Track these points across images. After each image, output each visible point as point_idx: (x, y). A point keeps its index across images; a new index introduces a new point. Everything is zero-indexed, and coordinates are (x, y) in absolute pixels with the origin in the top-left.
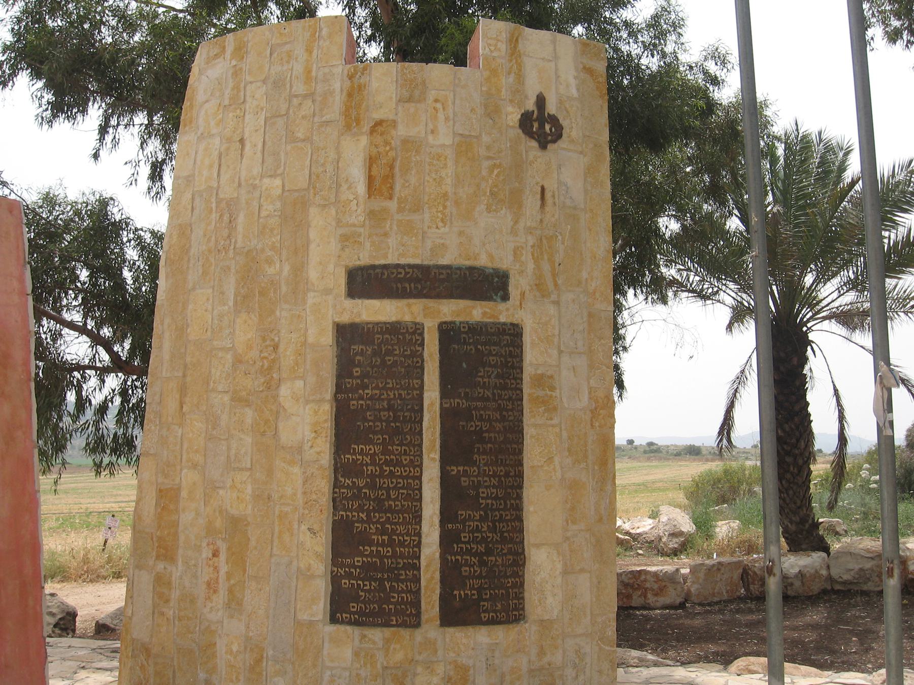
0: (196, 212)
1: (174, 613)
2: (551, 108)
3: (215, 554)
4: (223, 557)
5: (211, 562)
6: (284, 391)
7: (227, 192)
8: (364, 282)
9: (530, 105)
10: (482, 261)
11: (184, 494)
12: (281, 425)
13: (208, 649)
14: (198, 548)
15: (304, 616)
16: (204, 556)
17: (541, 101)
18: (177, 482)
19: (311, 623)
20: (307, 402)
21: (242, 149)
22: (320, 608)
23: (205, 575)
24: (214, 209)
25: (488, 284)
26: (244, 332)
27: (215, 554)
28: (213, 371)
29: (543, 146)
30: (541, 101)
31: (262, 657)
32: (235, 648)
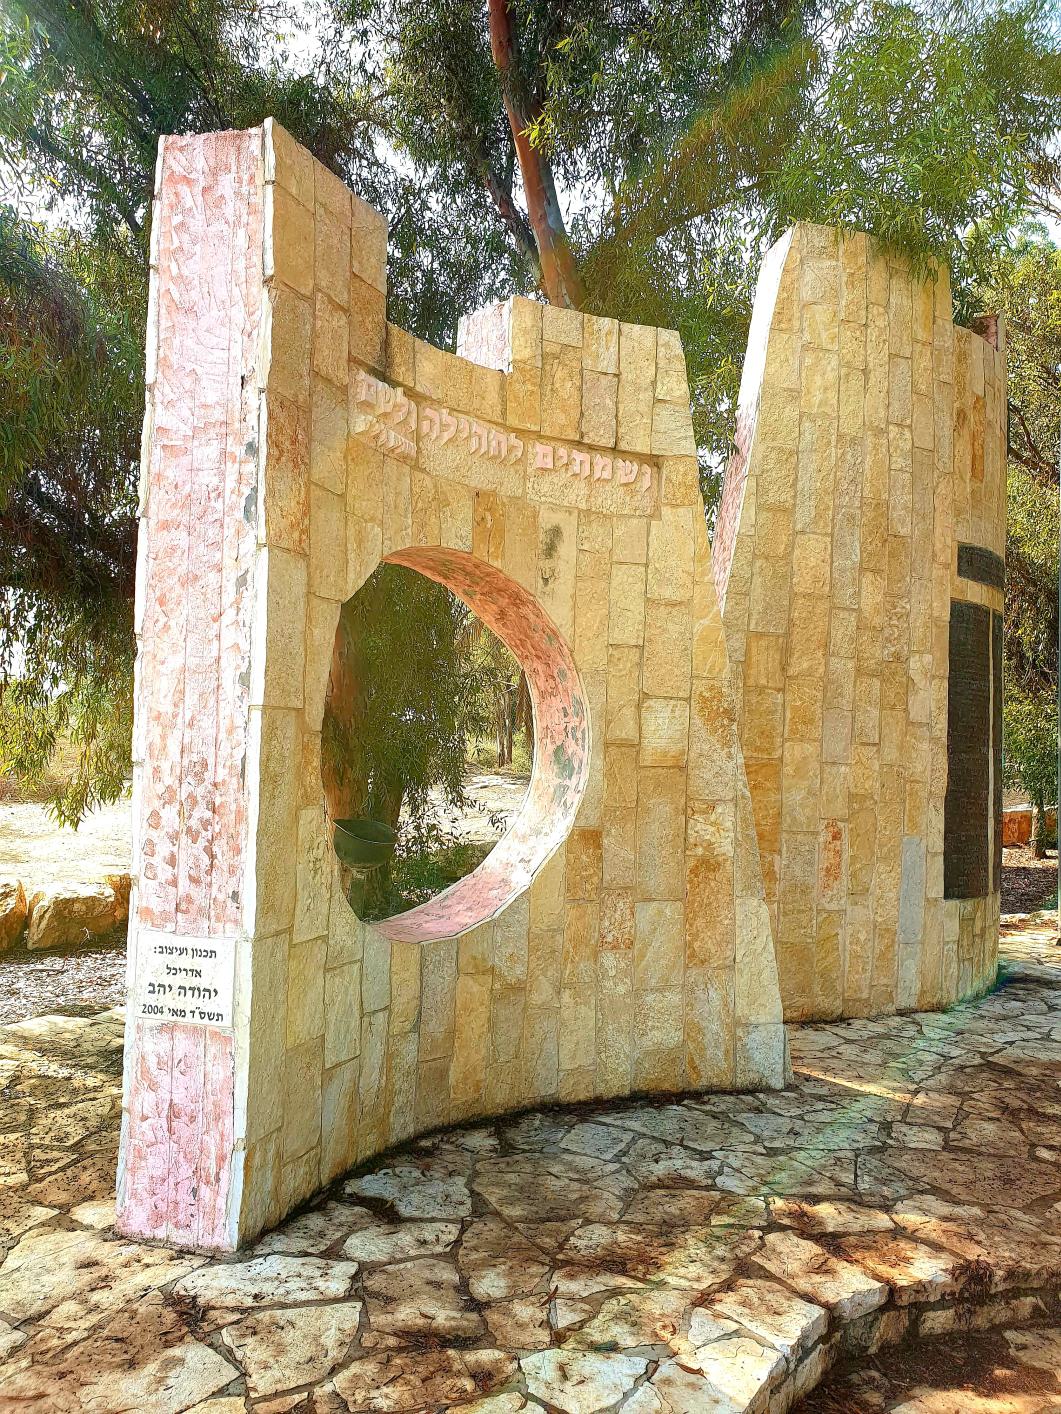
0: (807, 437)
1: (779, 908)
3: (836, 836)
4: (845, 836)
5: (832, 846)
6: (915, 664)
7: (850, 427)
11: (788, 770)
12: (911, 699)
13: (827, 941)
14: (815, 834)
15: (932, 895)
16: (821, 840)
18: (777, 754)
19: (936, 900)
20: (933, 677)
21: (867, 381)
23: (824, 860)
24: (833, 443)
26: (871, 595)
27: (836, 836)
28: (833, 633)
31: (893, 941)
32: (862, 937)
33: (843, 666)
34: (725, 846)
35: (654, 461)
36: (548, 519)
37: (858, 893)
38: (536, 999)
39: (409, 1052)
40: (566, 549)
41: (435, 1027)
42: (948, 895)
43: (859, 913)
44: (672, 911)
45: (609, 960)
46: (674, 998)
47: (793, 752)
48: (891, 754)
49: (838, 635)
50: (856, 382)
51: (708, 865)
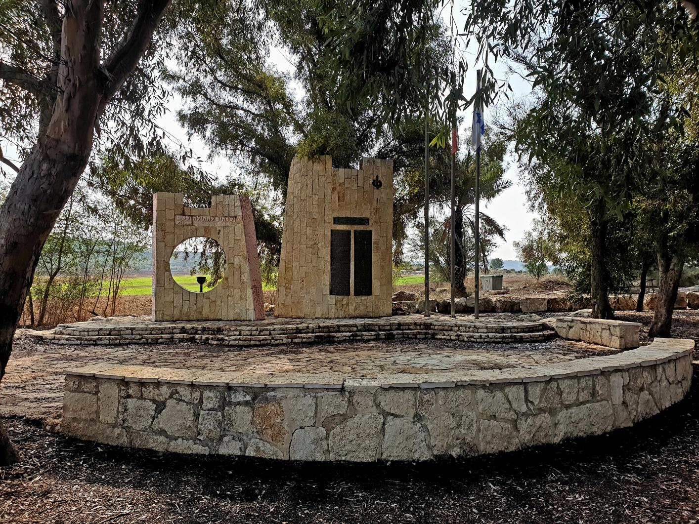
2: (380, 179)
8: (337, 221)
9: (375, 178)
10: (364, 216)
17: (377, 177)
22: (328, 291)
23: (301, 286)
25: (363, 221)
29: (378, 189)
30: (377, 177)
33: (303, 246)
34: (245, 280)
35: (236, 217)
36: (218, 229)
37: (307, 293)
38: (218, 303)
39: (194, 308)
40: (221, 233)
41: (199, 305)
42: (331, 293)
43: (308, 297)
44: (238, 290)
45: (229, 298)
46: (239, 305)
47: (294, 264)
48: (314, 264)
49: (302, 240)
50: (305, 187)
51: (243, 283)
